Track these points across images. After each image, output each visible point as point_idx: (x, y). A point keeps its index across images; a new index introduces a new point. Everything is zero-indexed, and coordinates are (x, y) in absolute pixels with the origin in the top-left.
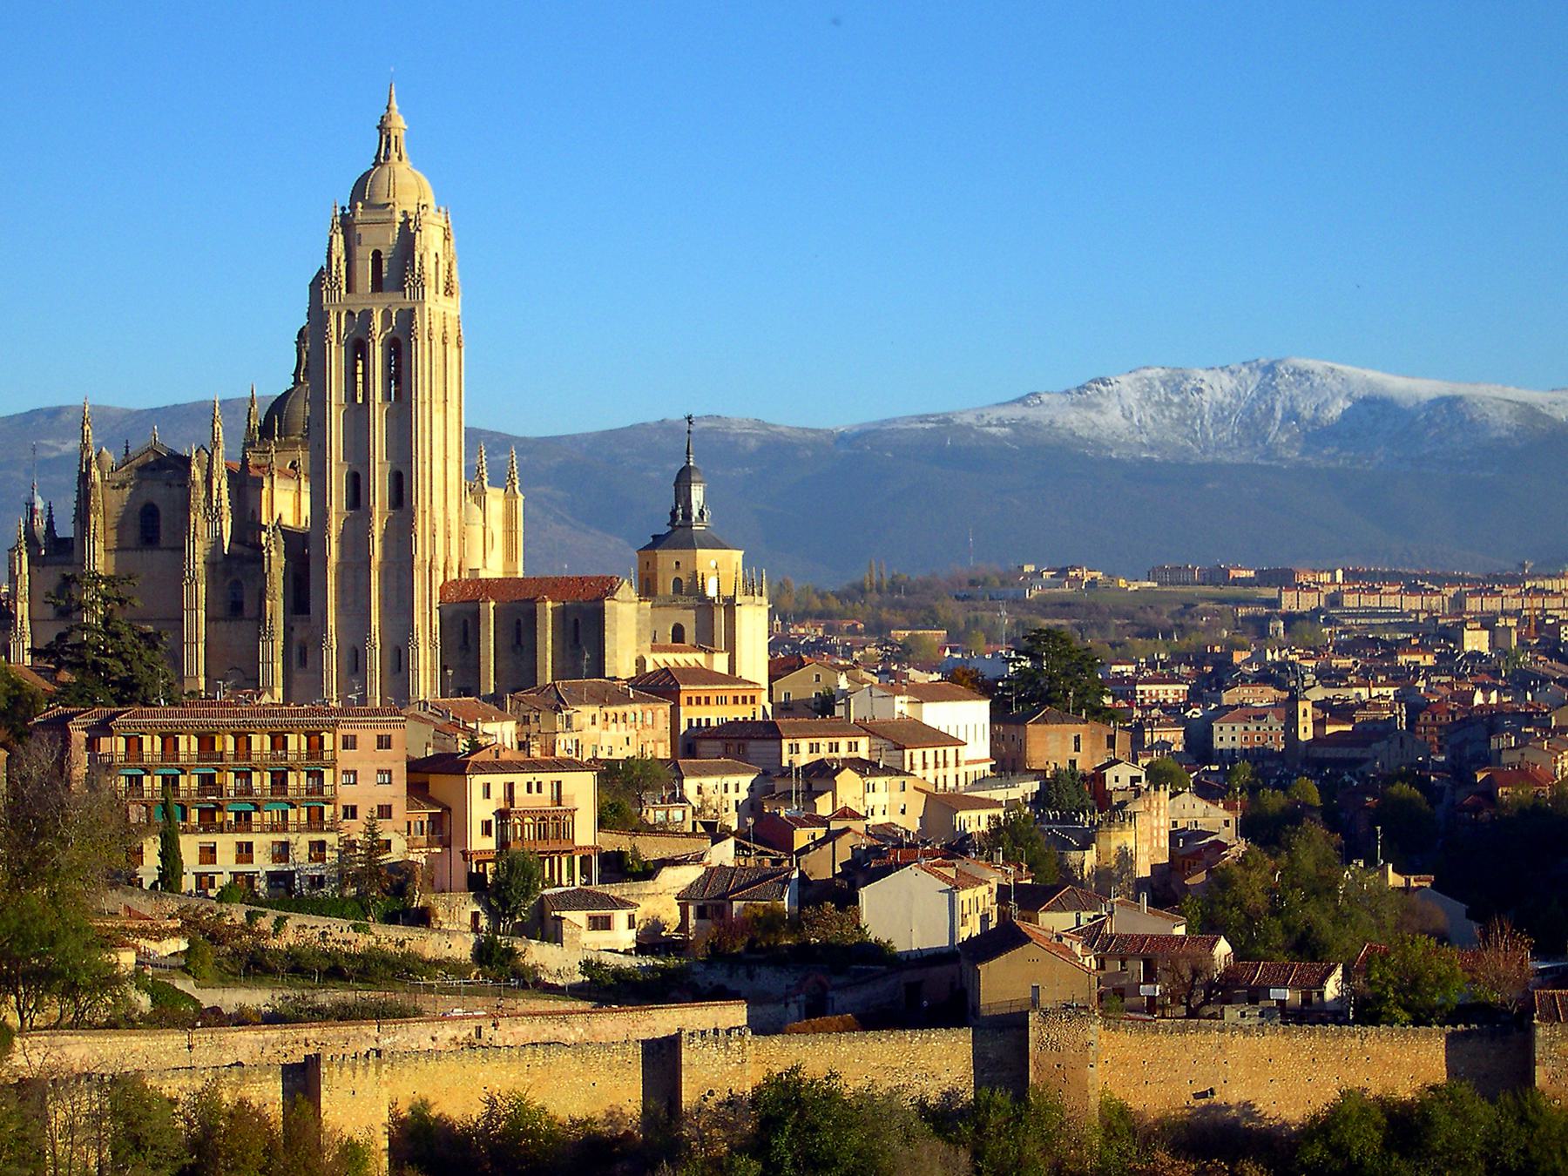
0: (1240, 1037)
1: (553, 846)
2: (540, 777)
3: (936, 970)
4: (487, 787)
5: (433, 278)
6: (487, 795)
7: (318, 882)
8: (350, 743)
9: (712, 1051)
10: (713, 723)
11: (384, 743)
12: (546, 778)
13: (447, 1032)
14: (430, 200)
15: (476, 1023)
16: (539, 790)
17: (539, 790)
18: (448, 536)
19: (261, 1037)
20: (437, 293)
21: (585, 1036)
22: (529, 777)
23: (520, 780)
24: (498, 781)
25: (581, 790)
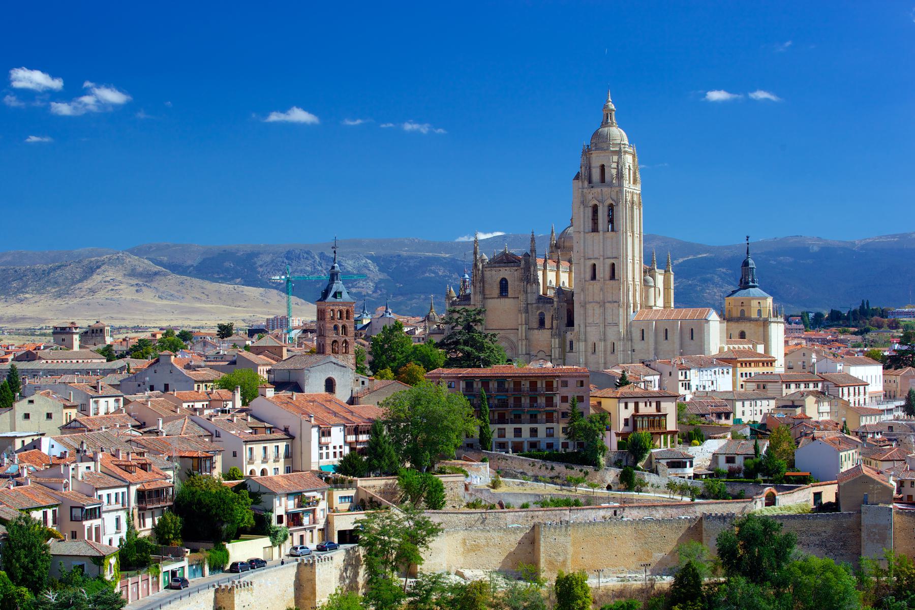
1: (657, 430)
2: (650, 399)
5: (628, 176)
6: (626, 407)
7: (550, 446)
8: (565, 384)
10: (753, 375)
13: (602, 513)
14: (626, 142)
16: (650, 406)
17: (650, 406)
18: (635, 291)
19: (517, 514)
20: (630, 183)
22: (646, 400)
25: (669, 408)
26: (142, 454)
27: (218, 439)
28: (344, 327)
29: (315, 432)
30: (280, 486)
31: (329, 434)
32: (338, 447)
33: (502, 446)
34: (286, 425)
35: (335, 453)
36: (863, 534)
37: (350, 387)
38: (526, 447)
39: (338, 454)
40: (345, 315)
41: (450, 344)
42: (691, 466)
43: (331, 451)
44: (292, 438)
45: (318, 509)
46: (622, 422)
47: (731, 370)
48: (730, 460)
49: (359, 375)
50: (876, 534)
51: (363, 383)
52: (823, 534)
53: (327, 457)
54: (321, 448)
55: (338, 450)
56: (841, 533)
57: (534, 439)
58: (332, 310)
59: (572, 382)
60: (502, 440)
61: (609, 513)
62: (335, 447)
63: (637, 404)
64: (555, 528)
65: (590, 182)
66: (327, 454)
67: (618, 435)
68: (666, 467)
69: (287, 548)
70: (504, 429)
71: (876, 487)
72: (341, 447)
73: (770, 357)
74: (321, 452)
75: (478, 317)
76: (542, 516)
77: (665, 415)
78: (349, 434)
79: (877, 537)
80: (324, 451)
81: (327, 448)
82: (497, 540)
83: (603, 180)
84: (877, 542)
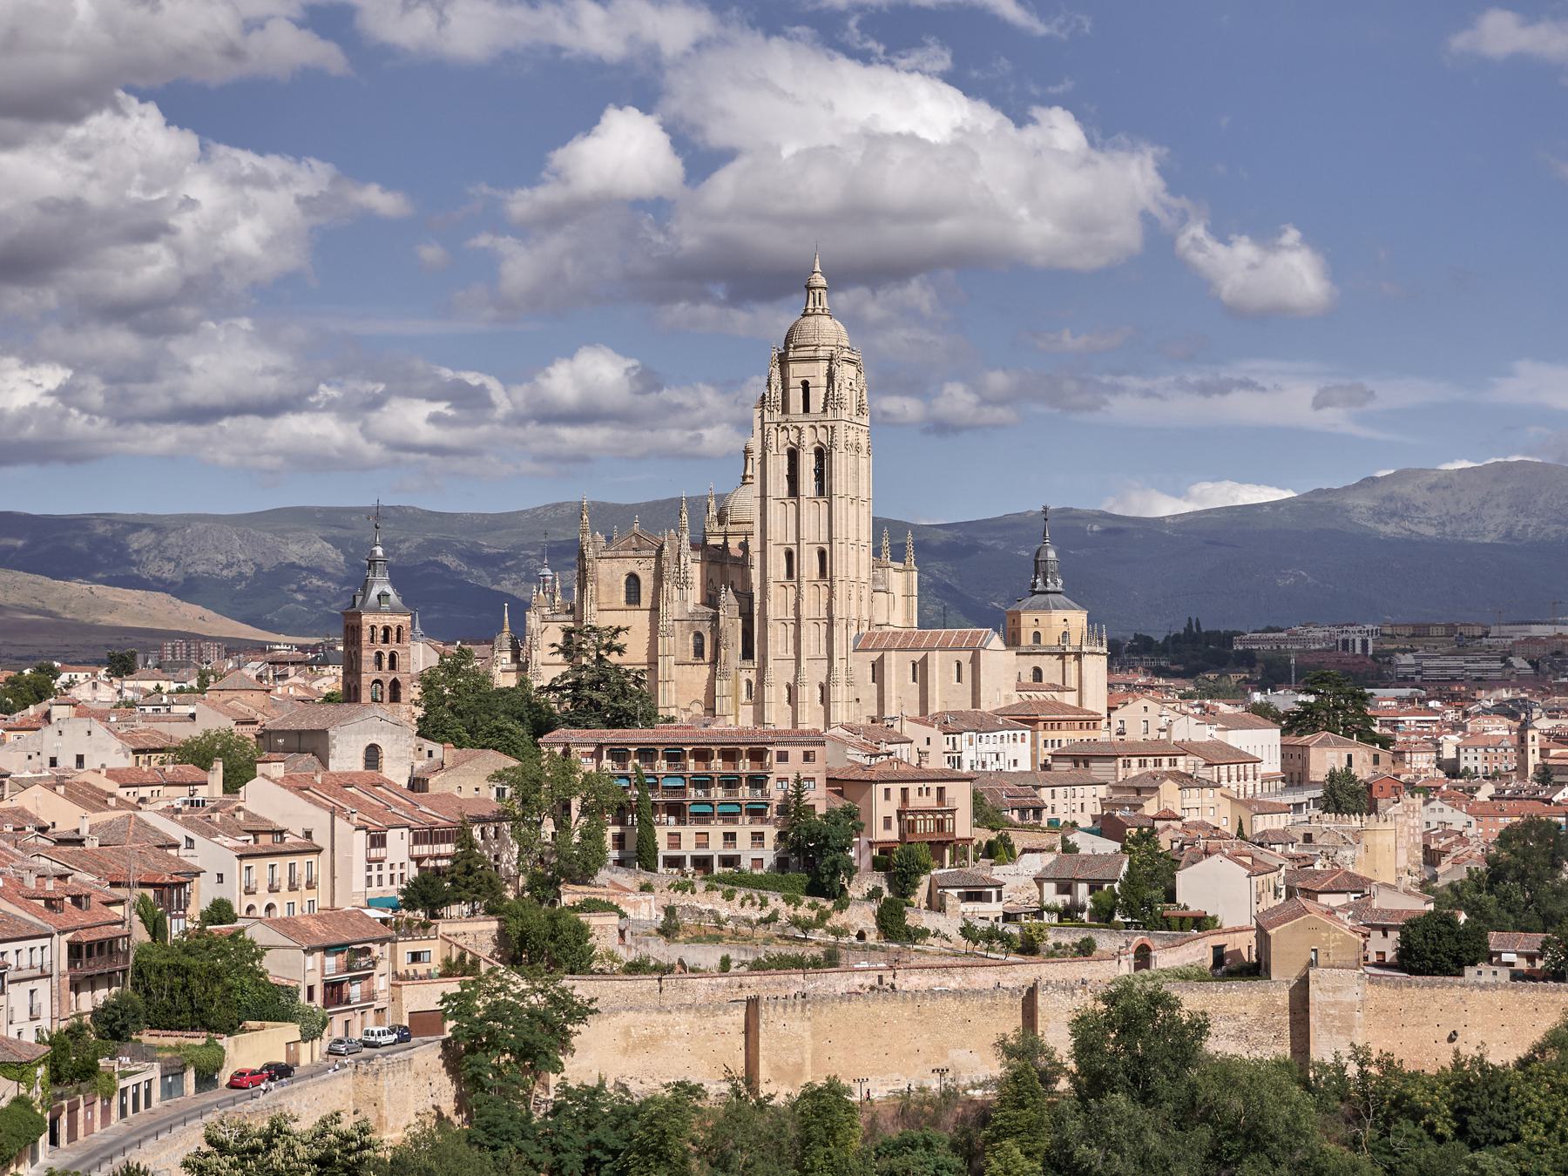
0: (1477, 991)
2: (928, 785)
3: (1238, 935)
4: (887, 790)
6: (887, 797)
7: (758, 862)
8: (783, 757)
9: (1060, 996)
10: (1064, 744)
11: (807, 757)
12: (934, 786)
13: (858, 979)
15: (879, 973)
19: (714, 982)
21: (963, 984)
22: (921, 785)
23: (913, 788)
24: (896, 789)
25: (960, 796)
26: (63, 877)
27: (190, 852)
28: (392, 657)
29: (361, 838)
30: (312, 935)
31: (383, 844)
32: (397, 866)
33: (674, 862)
34: (308, 827)
35: (392, 875)
36: (1312, 1019)
37: (408, 761)
38: (717, 869)
39: (397, 879)
40: (395, 636)
41: (564, 688)
42: (999, 898)
43: (386, 872)
44: (319, 851)
45: (376, 972)
46: (880, 823)
47: (1028, 733)
48: (1065, 887)
49: (423, 740)
50: (1335, 1018)
51: (430, 754)
52: (1242, 1018)
53: (380, 885)
54: (369, 869)
55: (397, 871)
56: (1273, 1015)
57: (730, 852)
58: (373, 627)
59: (796, 753)
60: (675, 853)
61: (874, 981)
62: (392, 866)
63: (904, 791)
64: (785, 1007)
65: (785, 409)
66: (380, 877)
67: (871, 844)
68: (958, 901)
69: (320, 1046)
70: (679, 834)
71: (1332, 937)
72: (402, 865)
73: (1093, 713)
74: (369, 874)
75: (615, 642)
76: (757, 984)
77: (952, 811)
78: (416, 842)
79: (1337, 1023)
80: (374, 873)
81: (380, 868)
82: (684, 1028)
83: (806, 409)
84: (1338, 1033)
